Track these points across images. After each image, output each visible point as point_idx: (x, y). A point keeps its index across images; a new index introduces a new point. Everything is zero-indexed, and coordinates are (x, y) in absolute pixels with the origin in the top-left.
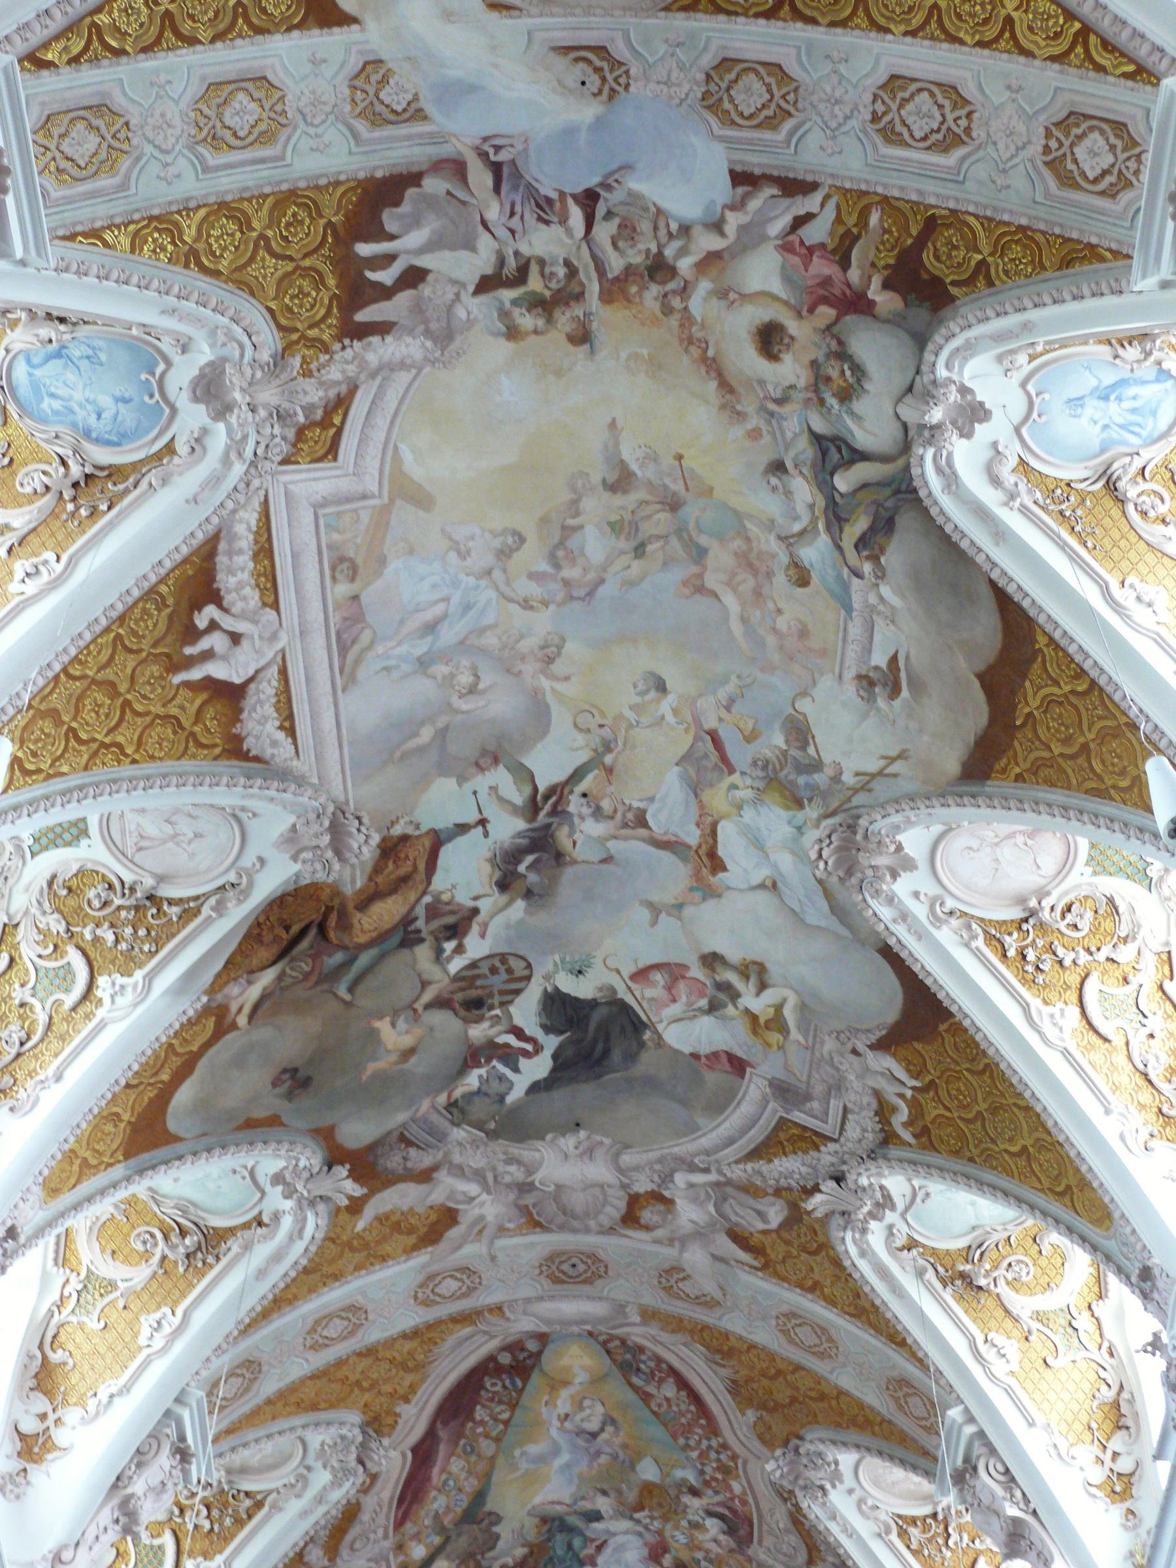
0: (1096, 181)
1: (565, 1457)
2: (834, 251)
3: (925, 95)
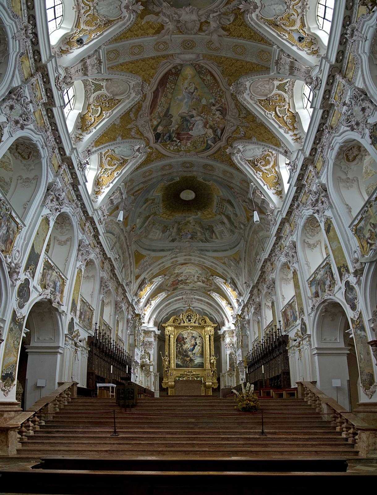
1: (186, 100)
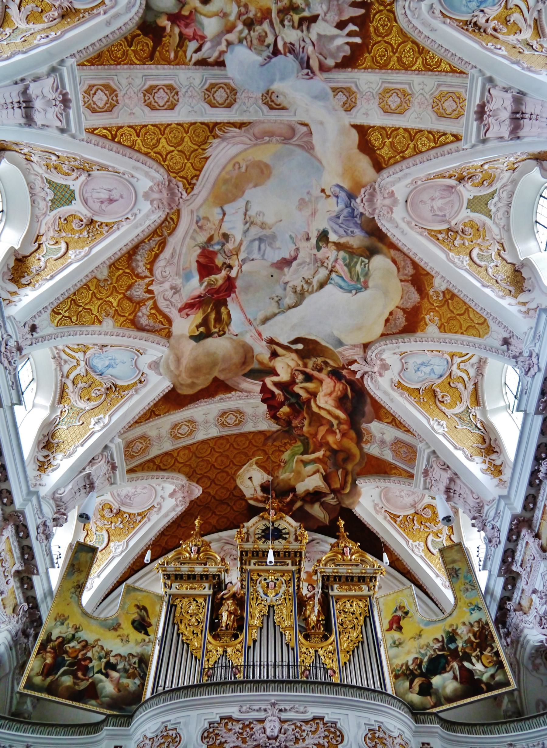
0: (97, 90)
2: (185, 39)
3: (161, 104)
